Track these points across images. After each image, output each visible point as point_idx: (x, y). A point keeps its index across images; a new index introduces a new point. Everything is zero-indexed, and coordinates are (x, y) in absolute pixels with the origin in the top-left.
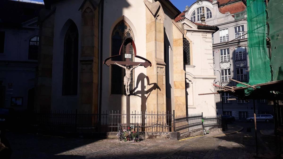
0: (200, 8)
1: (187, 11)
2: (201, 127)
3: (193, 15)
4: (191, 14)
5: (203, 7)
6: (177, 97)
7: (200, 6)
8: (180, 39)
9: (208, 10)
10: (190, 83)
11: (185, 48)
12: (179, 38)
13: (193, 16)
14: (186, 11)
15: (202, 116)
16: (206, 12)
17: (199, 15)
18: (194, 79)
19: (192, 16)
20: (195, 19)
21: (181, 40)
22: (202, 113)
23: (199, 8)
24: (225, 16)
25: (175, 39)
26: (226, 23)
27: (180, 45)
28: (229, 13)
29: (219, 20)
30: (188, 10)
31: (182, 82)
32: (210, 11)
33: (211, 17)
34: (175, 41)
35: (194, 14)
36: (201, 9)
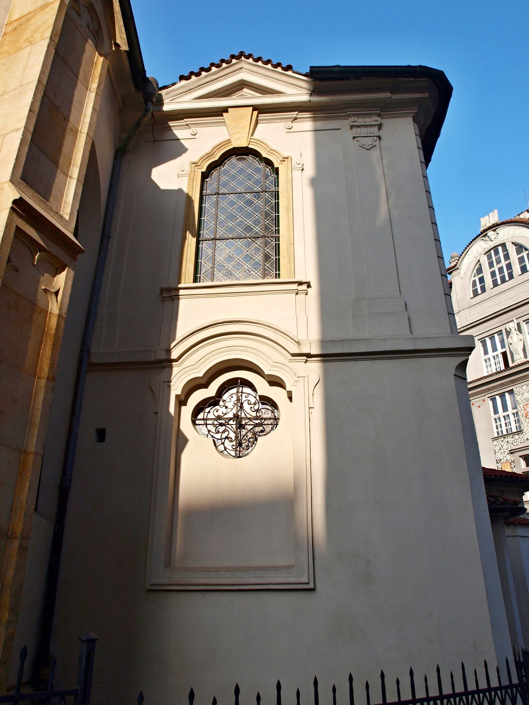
0: (495, 248)
1: (456, 265)
4: (469, 273)
5: (503, 245)
7: (492, 244)
9: (520, 248)
13: (477, 278)
14: (453, 267)
17: (494, 271)
19: (473, 279)
23: (490, 250)
35: (480, 270)
36: (497, 253)
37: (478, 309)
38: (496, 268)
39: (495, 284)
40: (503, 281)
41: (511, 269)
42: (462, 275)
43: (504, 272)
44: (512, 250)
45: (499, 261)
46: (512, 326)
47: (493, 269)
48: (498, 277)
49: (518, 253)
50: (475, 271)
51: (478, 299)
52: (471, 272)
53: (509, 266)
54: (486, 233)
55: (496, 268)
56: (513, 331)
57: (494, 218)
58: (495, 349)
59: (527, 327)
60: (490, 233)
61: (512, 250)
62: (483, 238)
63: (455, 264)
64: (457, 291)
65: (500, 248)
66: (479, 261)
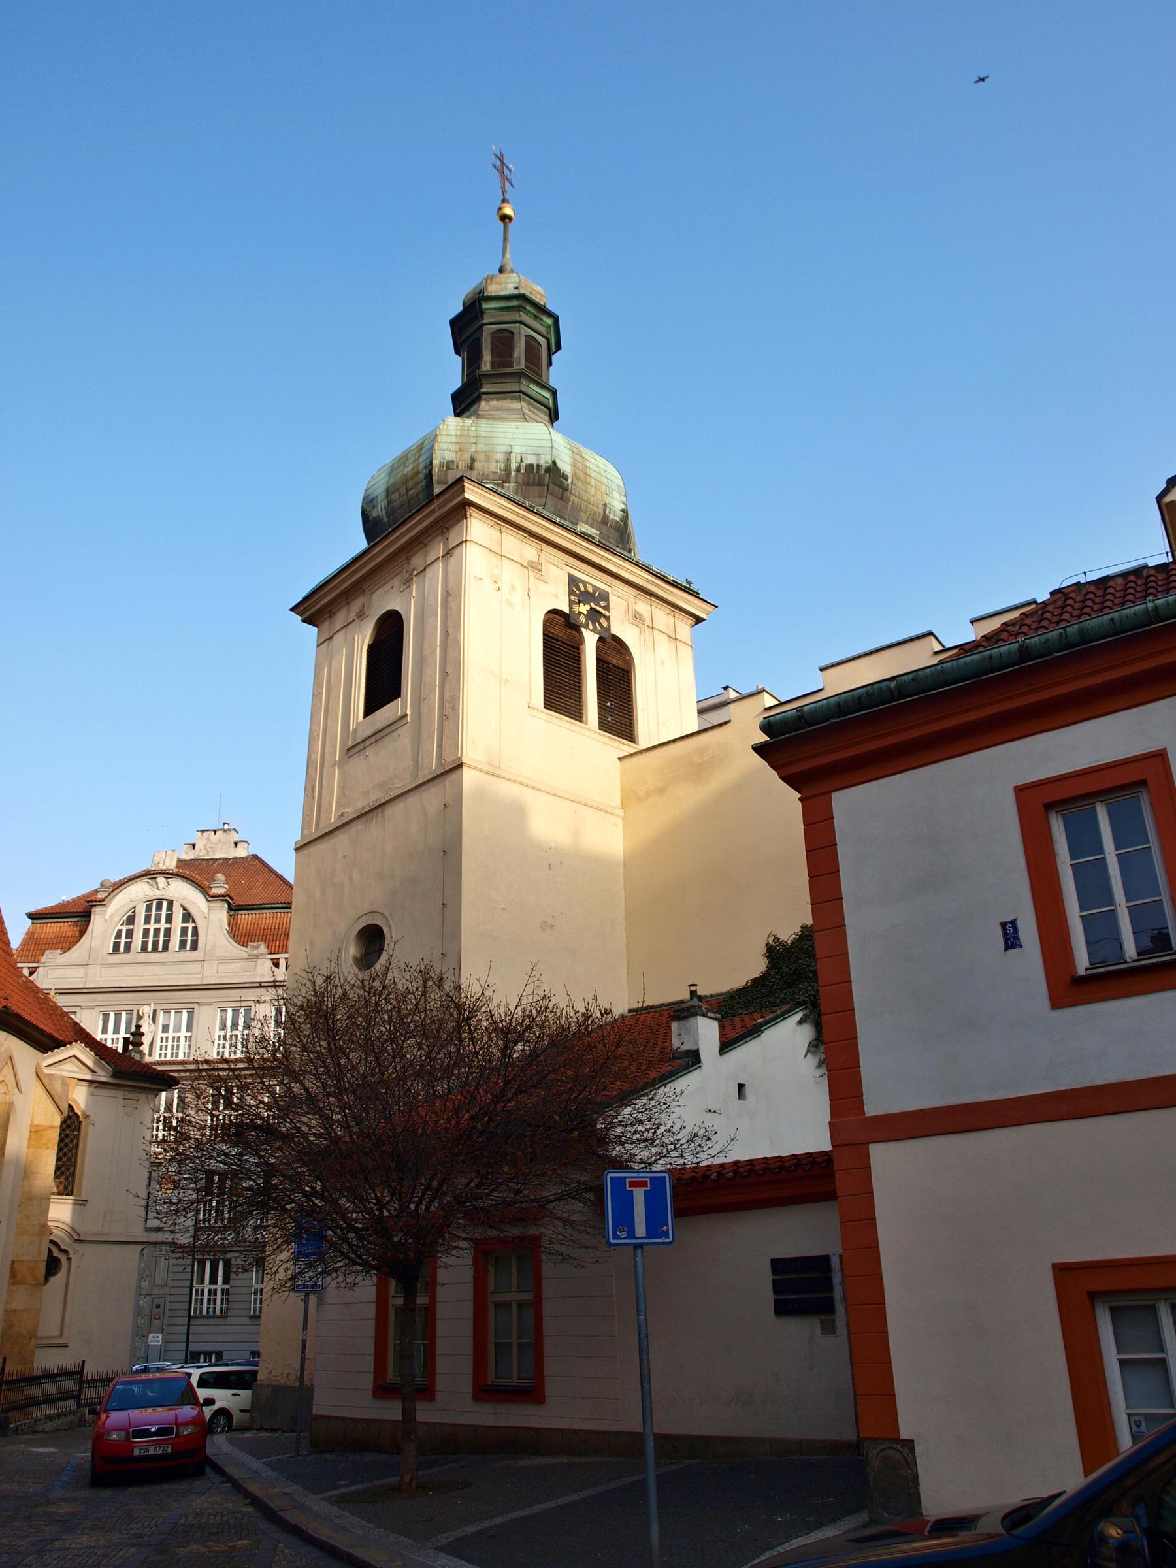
2: (71, 1405)
3: (127, 924)
4: (117, 919)
5: (170, 904)
6: (15, 1311)
7: (158, 894)
8: (52, 1127)
9: (187, 916)
10: (63, 1258)
11: (63, 1135)
12: (48, 1124)
13: (124, 929)
14: (100, 901)
15: (81, 1372)
16: (178, 924)
18: (78, 1246)
19: (119, 927)
20: (131, 942)
21: (54, 1130)
22: (84, 1362)
24: (245, 955)
25: (37, 1126)
26: (247, 985)
27: (50, 1145)
28: (263, 948)
29: (222, 967)
30: (106, 897)
31: (36, 1262)
32: (194, 921)
33: (195, 946)
34: (36, 1132)
35: (131, 920)
36: (159, 908)
37: (113, 971)
38: (152, 927)
39: (144, 948)
40: (155, 948)
41: (169, 937)
42: (107, 917)
43: (159, 937)
44: (178, 914)
45: (158, 921)
46: (147, 1010)
47: (147, 926)
48: (151, 939)
49: (184, 921)
50: (125, 918)
51: (117, 958)
52: (119, 918)
53: (168, 932)
54: (156, 876)
55: (152, 927)
56: (146, 1017)
57: (171, 860)
58: (116, 1030)
59: (164, 1016)
60: (161, 880)
61: (178, 914)
62: (150, 881)
63: (103, 896)
64: (94, 935)
65: (165, 904)
66: (135, 907)
